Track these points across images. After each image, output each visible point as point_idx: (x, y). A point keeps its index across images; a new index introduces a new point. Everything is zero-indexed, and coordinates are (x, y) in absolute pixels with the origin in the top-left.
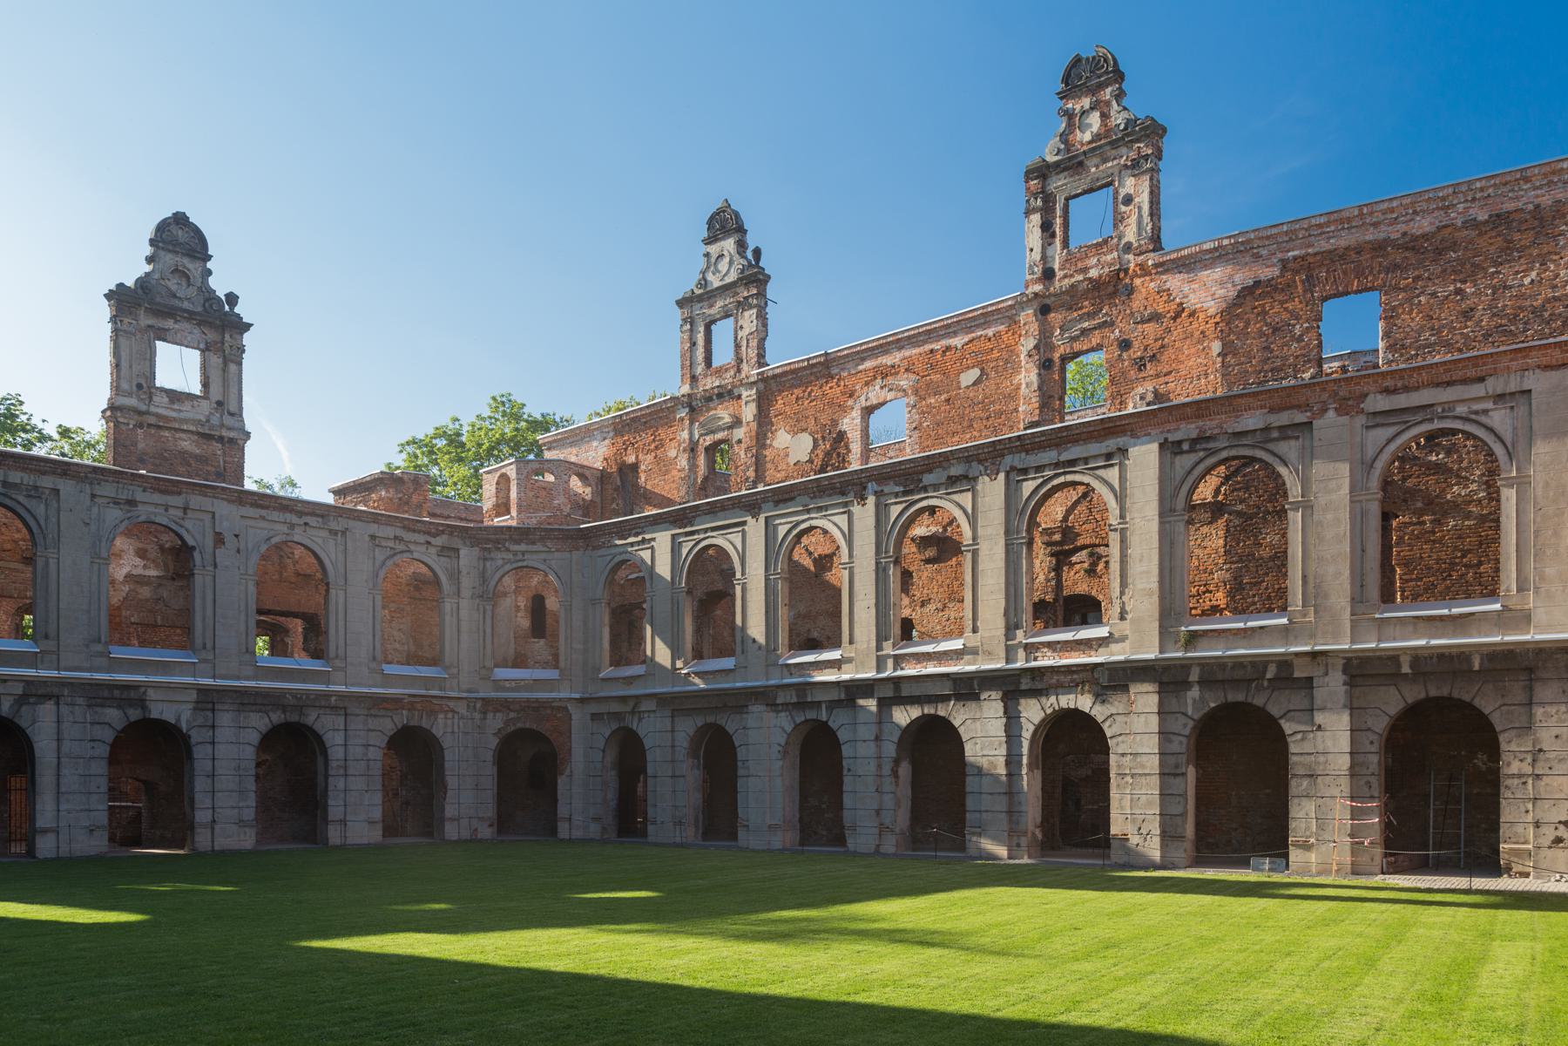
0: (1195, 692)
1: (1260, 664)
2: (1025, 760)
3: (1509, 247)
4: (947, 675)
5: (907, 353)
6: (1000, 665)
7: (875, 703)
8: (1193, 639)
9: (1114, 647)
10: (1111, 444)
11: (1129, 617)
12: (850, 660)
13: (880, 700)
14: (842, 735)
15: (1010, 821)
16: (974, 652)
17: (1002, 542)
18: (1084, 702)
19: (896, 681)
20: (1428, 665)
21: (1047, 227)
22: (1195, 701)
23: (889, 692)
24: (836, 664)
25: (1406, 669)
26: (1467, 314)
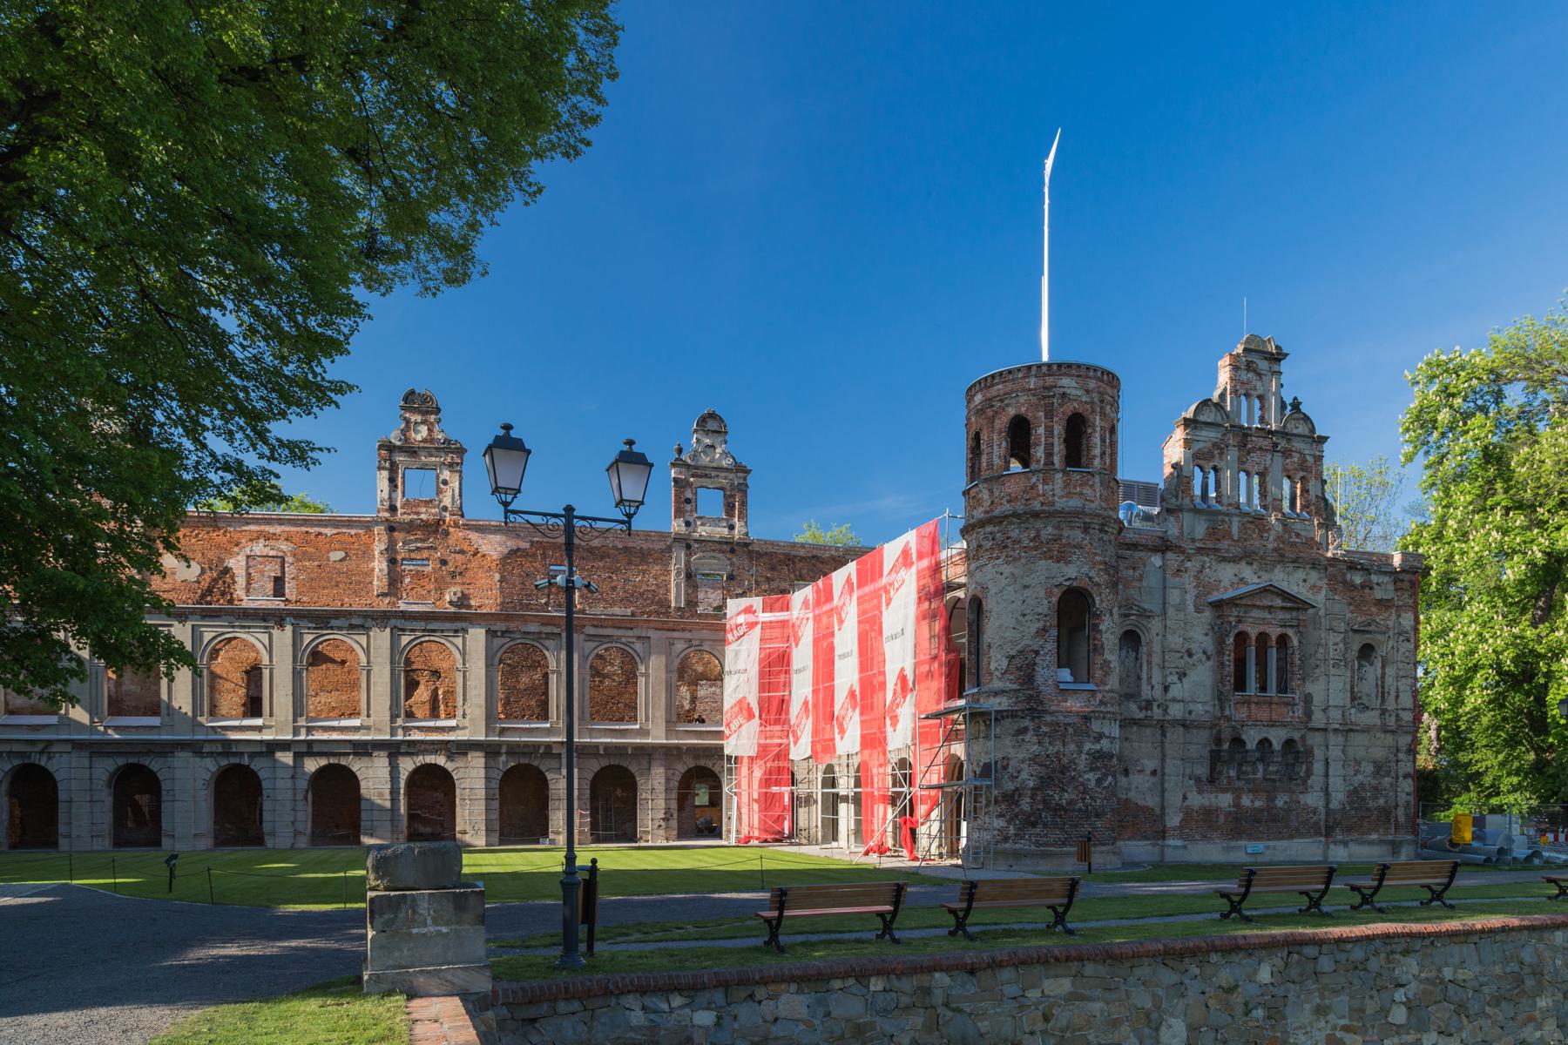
1: (536, 746)
2: (402, 791)
3: (630, 563)
4: (350, 741)
5: (288, 528)
6: (388, 737)
7: (291, 754)
8: (503, 731)
9: (459, 732)
10: (458, 625)
11: (468, 717)
12: (270, 727)
13: (295, 753)
14: (262, 775)
15: (392, 825)
16: (368, 728)
17: (388, 668)
19: (310, 743)
20: (611, 750)
21: (392, 480)
23: (304, 749)
24: (259, 729)
25: (602, 752)
26: (614, 588)
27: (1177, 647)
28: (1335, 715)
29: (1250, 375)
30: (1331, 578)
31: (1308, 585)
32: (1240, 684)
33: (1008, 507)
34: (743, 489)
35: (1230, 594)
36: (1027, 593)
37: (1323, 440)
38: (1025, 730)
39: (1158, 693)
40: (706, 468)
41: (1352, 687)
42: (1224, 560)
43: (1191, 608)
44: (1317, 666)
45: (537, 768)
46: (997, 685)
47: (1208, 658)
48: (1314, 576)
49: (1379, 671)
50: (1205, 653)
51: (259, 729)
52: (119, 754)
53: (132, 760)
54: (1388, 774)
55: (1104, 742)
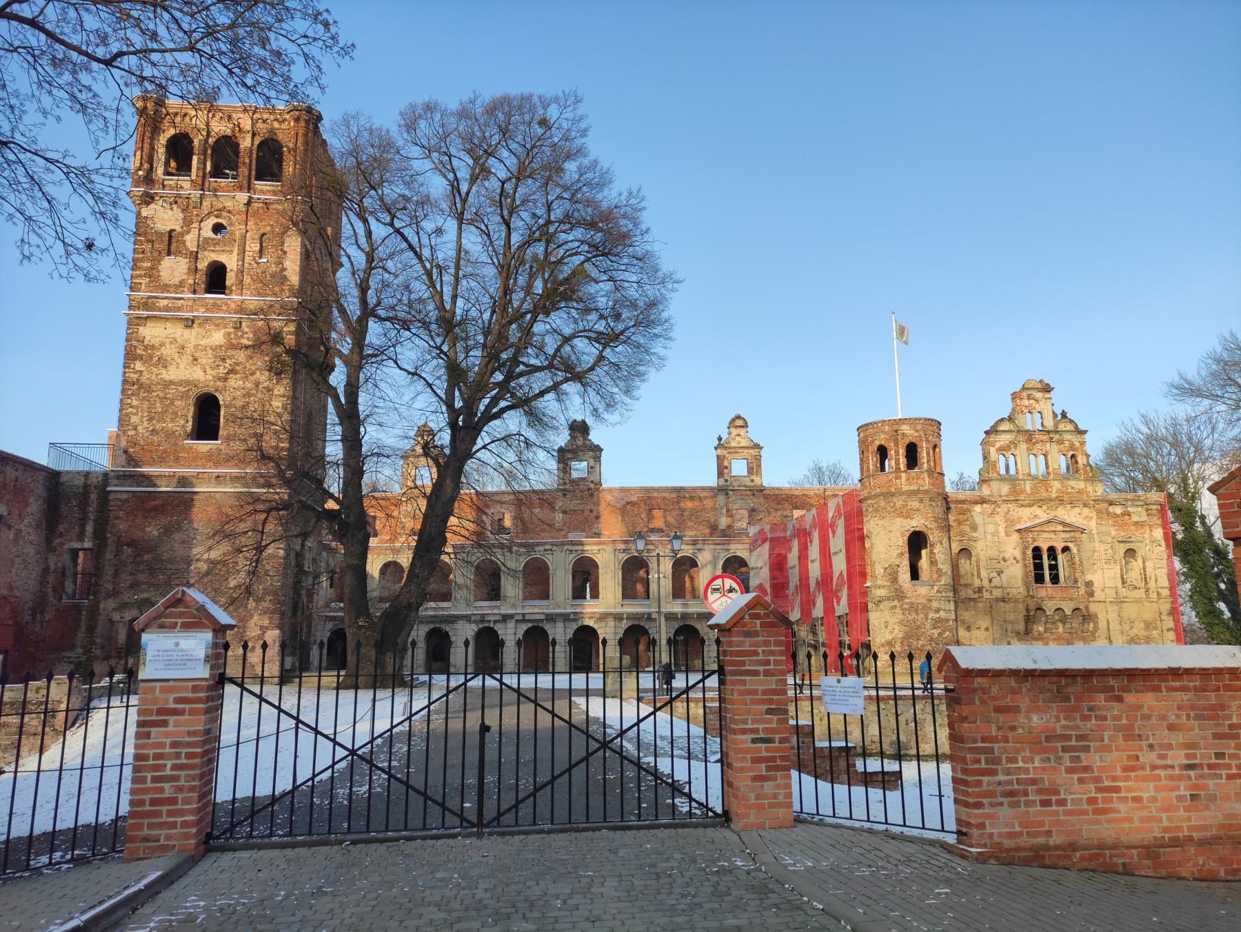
0: (625, 621)
18: (590, 623)
19: (524, 615)
20: (685, 616)
22: (625, 624)
23: (520, 617)
27: (995, 557)
28: (1112, 593)
29: (1031, 401)
30: (1099, 512)
31: (1082, 516)
32: (1039, 579)
33: (878, 491)
34: (758, 459)
35: (1029, 524)
36: (892, 535)
37: (1084, 432)
38: (895, 607)
39: (986, 583)
40: (735, 448)
41: (1122, 576)
42: (1022, 506)
43: (1003, 534)
44: (1094, 564)
45: (643, 627)
46: (879, 582)
47: (1018, 562)
48: (1086, 511)
49: (1141, 565)
50: (1015, 558)
51: (499, 607)
52: (432, 622)
53: (438, 626)
54: (1156, 628)
55: (941, 613)
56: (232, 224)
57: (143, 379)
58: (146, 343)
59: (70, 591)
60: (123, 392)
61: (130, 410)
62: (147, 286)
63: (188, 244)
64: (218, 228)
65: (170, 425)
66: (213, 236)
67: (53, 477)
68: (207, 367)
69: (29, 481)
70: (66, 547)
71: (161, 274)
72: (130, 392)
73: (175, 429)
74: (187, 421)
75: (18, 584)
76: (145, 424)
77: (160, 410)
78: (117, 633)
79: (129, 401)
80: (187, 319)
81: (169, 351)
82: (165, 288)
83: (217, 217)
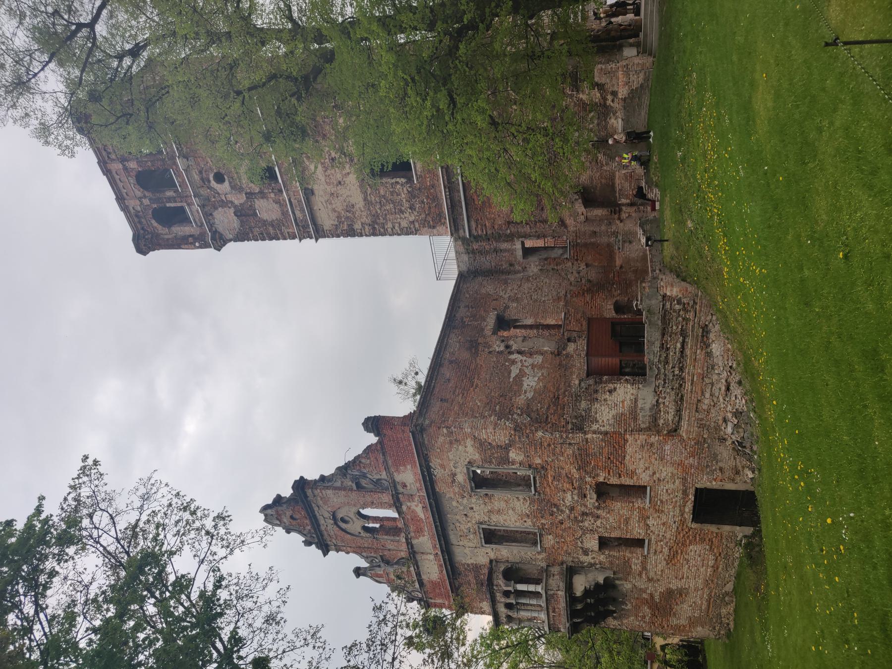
56: (211, 169)
57: (368, 221)
58: (336, 223)
59: (560, 251)
60: (382, 235)
61: (396, 228)
62: (288, 227)
63: (242, 201)
64: (219, 178)
65: (403, 196)
66: (227, 183)
67: (462, 278)
68: (344, 172)
69: (468, 296)
70: (521, 260)
71: (274, 218)
72: (382, 230)
73: (406, 192)
74: (397, 183)
75: (555, 293)
76: (407, 215)
77: (392, 205)
78: (596, 216)
79: (390, 230)
80: (305, 194)
81: (339, 205)
82: (285, 214)
83: (209, 181)
